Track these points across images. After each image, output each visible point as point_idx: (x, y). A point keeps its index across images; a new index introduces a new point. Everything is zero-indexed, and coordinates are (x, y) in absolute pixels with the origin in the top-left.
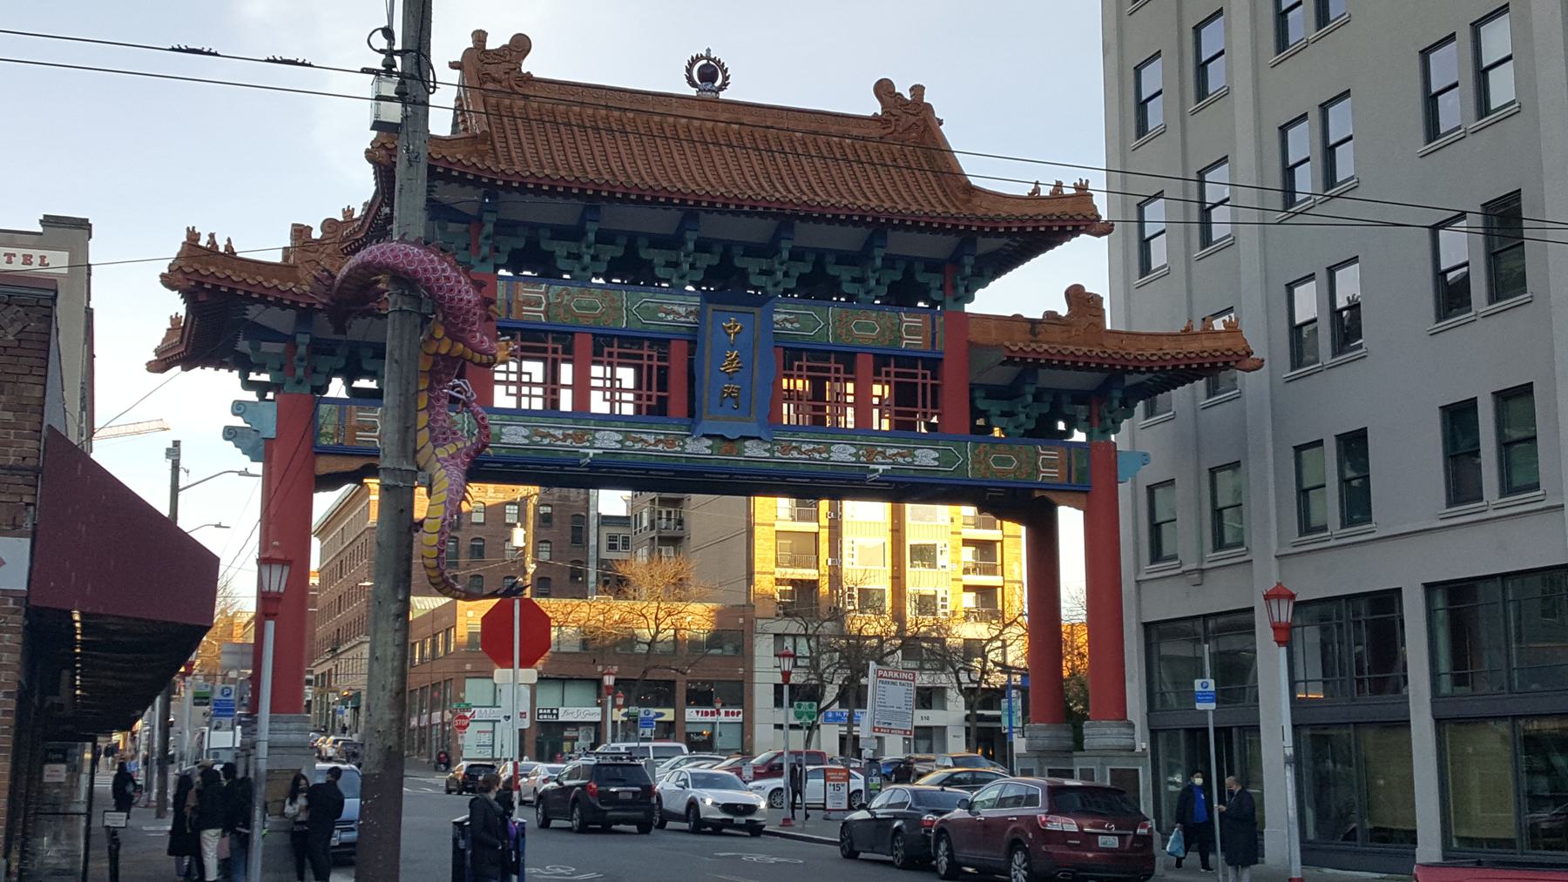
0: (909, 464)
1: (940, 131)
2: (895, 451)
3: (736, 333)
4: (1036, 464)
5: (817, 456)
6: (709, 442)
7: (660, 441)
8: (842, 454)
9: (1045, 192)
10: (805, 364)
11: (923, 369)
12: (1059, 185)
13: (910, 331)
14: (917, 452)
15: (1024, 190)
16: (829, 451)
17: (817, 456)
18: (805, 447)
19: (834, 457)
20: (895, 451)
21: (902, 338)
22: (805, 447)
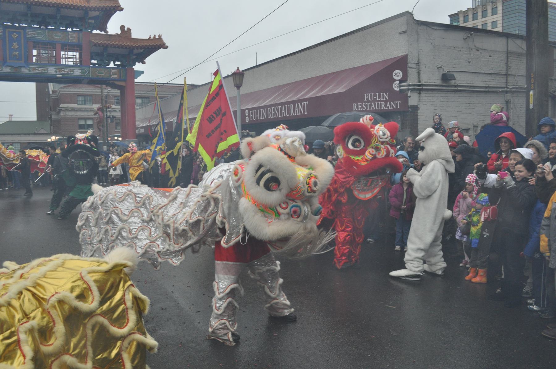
0: (72, 73)
2: (68, 70)
3: (16, 38)
4: (110, 73)
5: (44, 71)
6: (10, 68)
8: (51, 71)
10: (40, 46)
11: (77, 47)
13: (72, 37)
14: (75, 70)
17: (44, 71)
18: (40, 69)
19: (49, 72)
20: (68, 70)
21: (69, 39)
22: (40, 69)
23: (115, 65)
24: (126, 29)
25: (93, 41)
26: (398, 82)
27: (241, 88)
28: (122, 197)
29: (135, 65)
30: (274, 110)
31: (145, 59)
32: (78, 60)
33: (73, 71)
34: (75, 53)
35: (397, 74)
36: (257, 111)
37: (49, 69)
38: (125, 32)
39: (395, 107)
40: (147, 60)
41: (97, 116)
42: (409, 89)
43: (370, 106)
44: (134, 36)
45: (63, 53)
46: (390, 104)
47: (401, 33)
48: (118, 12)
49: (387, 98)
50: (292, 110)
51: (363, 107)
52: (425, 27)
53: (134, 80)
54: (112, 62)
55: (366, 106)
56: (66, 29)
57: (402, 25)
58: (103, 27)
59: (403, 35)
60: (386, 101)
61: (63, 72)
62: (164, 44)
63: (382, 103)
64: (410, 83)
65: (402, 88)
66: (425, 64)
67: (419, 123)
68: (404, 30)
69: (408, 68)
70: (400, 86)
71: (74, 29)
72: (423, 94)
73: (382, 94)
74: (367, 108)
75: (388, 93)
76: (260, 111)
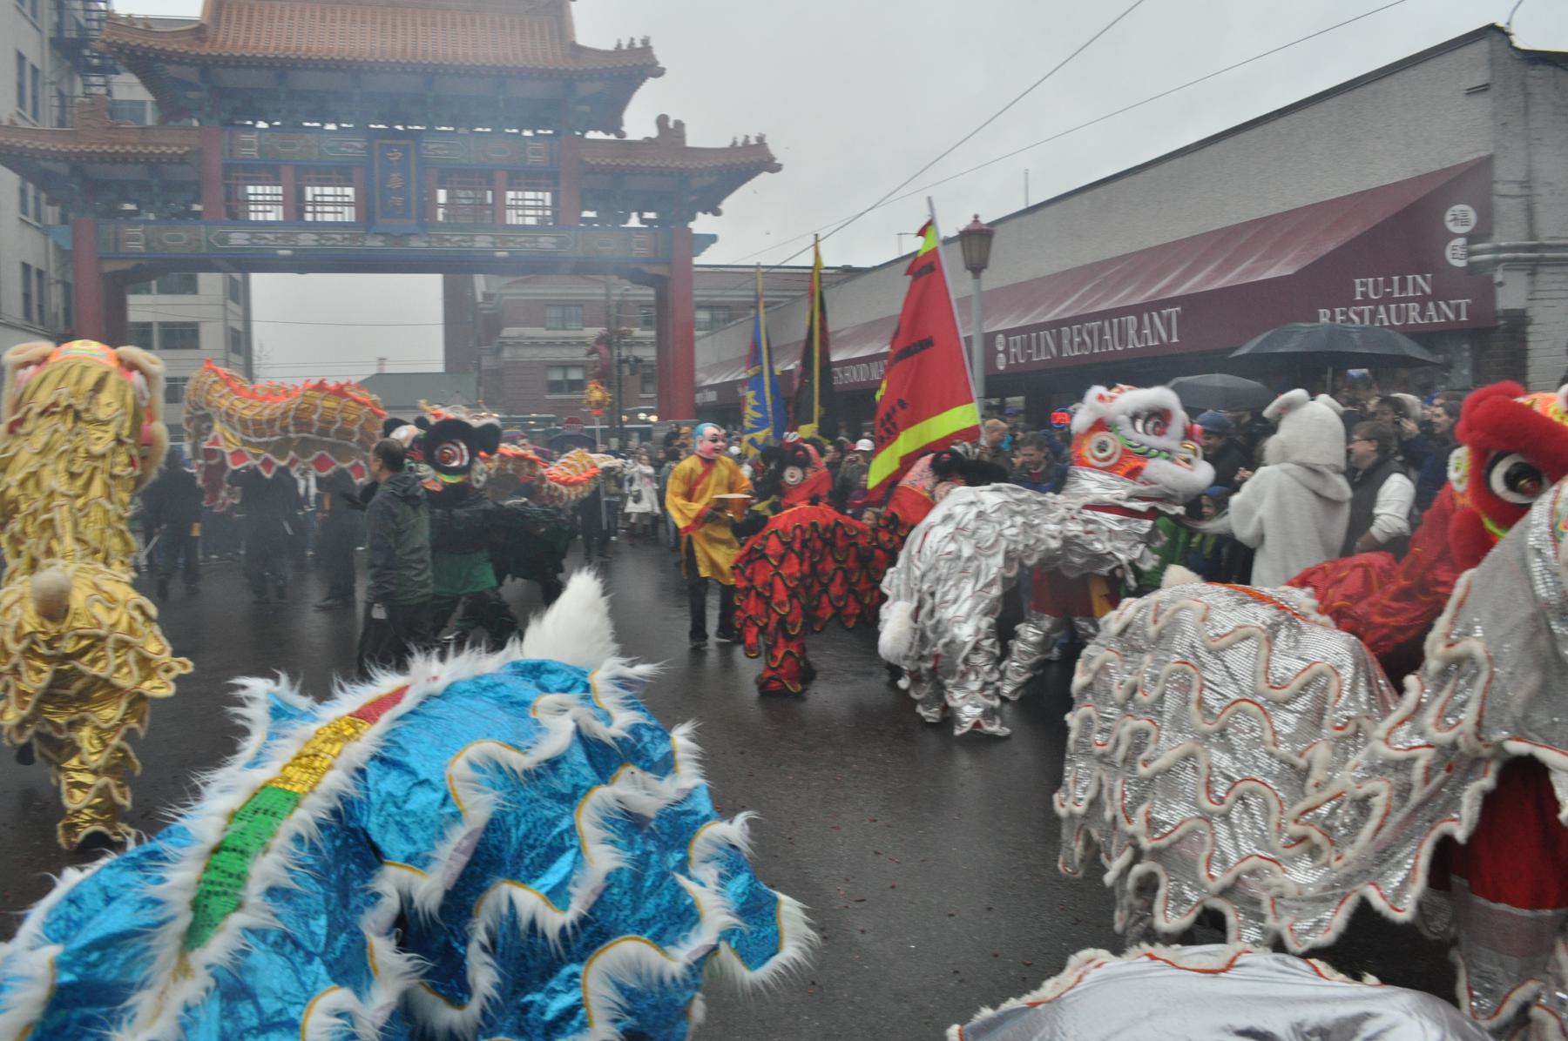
1: (569, 7)
2: (523, 239)
6: (381, 238)
7: (345, 239)
8: (482, 242)
9: (624, 47)
12: (632, 39)
14: (541, 239)
15: (611, 46)
16: (472, 240)
19: (478, 245)
20: (523, 239)
23: (643, 221)
24: (671, 124)
25: (588, 159)
26: (1461, 241)
27: (985, 273)
28: (1226, 635)
29: (693, 218)
30: (1080, 333)
31: (720, 203)
32: (548, 213)
33: (536, 242)
34: (540, 195)
35: (1460, 217)
36: (1029, 338)
37: (477, 238)
38: (670, 132)
39: (1452, 316)
40: (722, 207)
41: (595, 357)
42: (1497, 262)
43: (1373, 314)
44: (693, 140)
45: (510, 195)
46: (1438, 308)
47: (1472, 92)
48: (651, 82)
49: (1428, 290)
50: (1132, 332)
51: (1350, 320)
52: (1550, 70)
53: (690, 261)
54: (634, 215)
55: (1360, 315)
56: (521, 131)
57: (1474, 67)
58: (613, 123)
59: (1481, 100)
60: (1423, 301)
61: (512, 245)
62: (772, 159)
63: (1410, 305)
64: (1503, 244)
65: (1476, 258)
66: (1550, 184)
67: (1530, 362)
68: (1479, 78)
69: (1495, 198)
70: (1471, 253)
71: (540, 132)
72: (1545, 277)
73: (1410, 277)
74: (1362, 321)
75: (1428, 275)
76: (1038, 337)
